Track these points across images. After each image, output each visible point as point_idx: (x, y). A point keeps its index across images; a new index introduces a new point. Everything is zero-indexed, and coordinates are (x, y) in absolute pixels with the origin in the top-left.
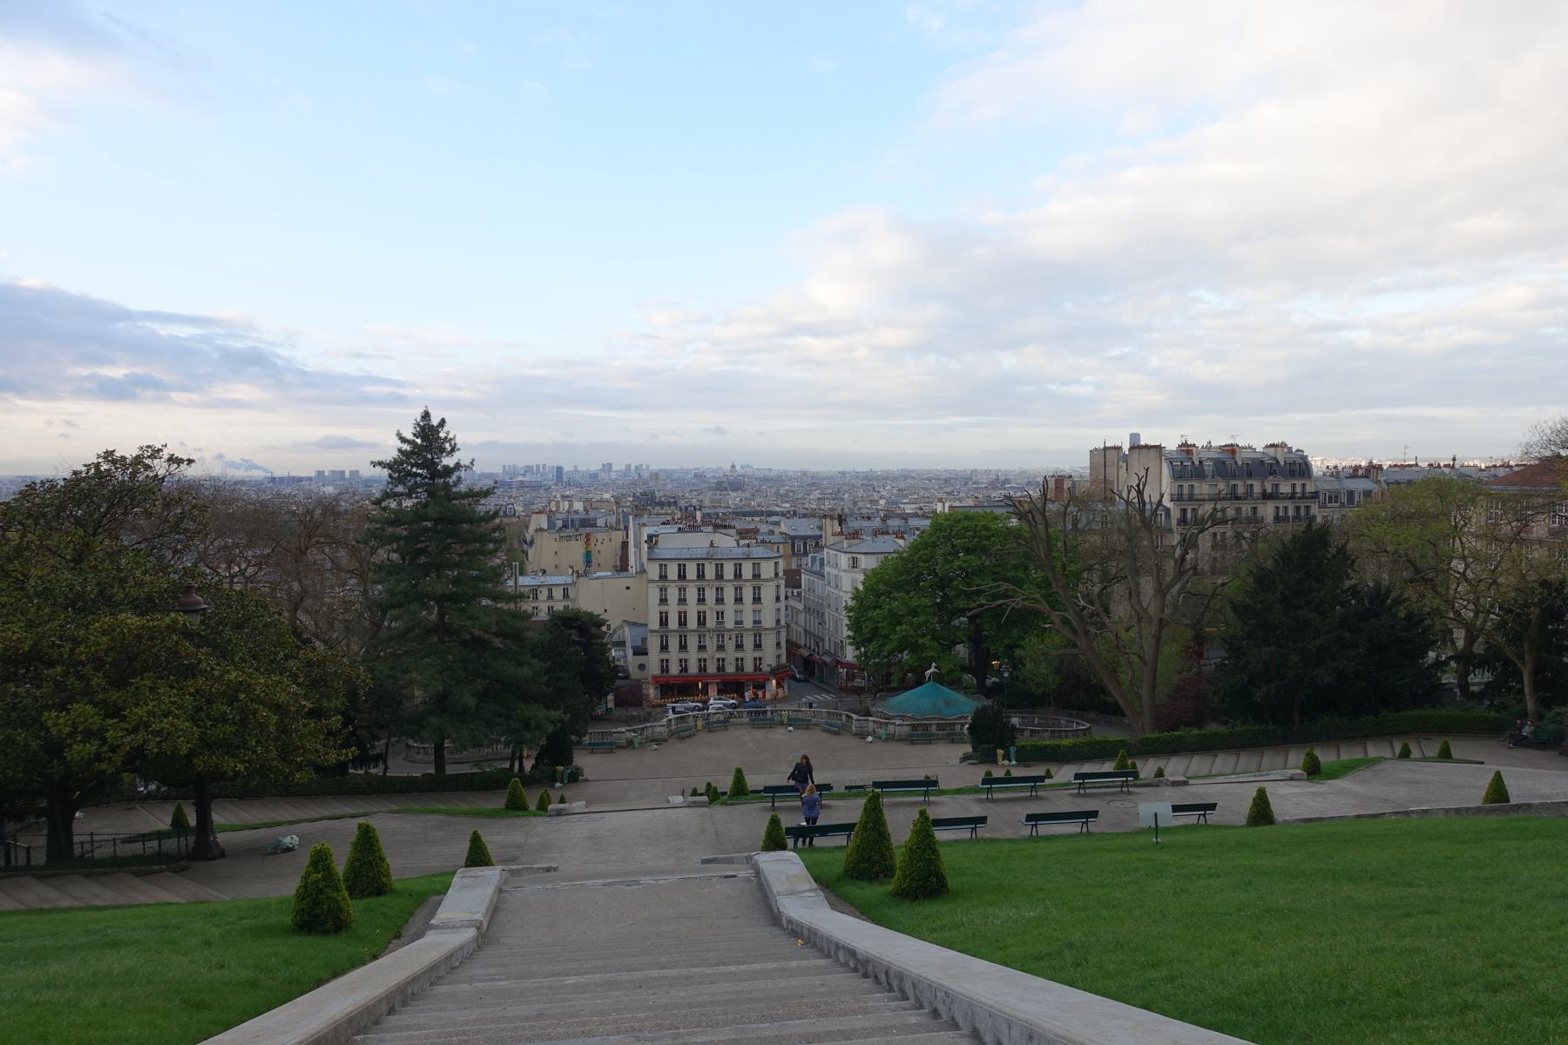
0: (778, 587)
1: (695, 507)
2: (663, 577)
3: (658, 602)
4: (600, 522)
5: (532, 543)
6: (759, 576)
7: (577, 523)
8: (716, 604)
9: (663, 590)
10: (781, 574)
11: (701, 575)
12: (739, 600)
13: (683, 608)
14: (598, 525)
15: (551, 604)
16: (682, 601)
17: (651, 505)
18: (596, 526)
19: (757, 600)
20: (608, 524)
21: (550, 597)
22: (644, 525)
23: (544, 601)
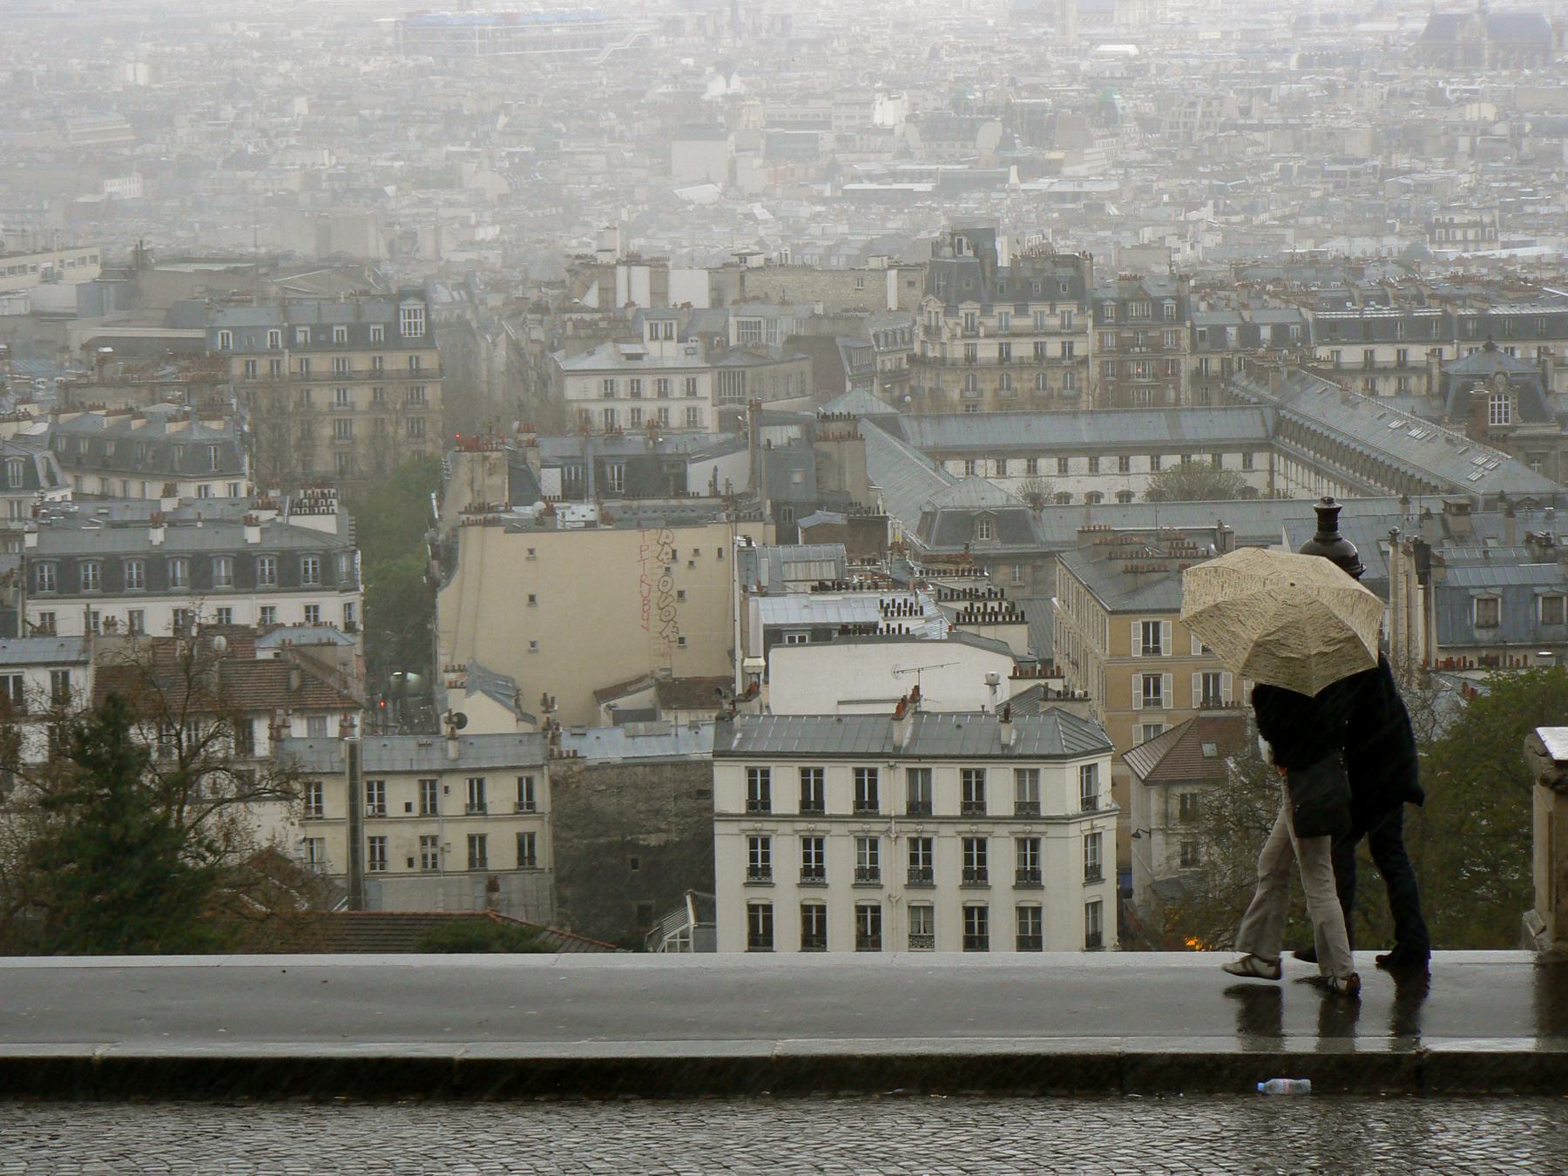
0: (1094, 838)
1: (1157, 304)
2: (759, 804)
3: (743, 876)
4: (698, 476)
5: (448, 557)
6: (1035, 806)
7: (612, 473)
8: (908, 886)
9: (759, 849)
10: (1105, 800)
11: (866, 803)
12: (975, 874)
13: (812, 896)
14: (692, 487)
15: (476, 827)
16: (813, 872)
17: (974, 296)
18: (686, 495)
19: (1029, 877)
20: (722, 489)
21: (477, 805)
22: (763, 592)
23: (453, 819)
